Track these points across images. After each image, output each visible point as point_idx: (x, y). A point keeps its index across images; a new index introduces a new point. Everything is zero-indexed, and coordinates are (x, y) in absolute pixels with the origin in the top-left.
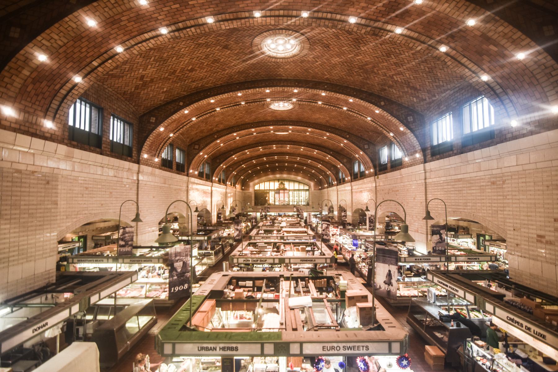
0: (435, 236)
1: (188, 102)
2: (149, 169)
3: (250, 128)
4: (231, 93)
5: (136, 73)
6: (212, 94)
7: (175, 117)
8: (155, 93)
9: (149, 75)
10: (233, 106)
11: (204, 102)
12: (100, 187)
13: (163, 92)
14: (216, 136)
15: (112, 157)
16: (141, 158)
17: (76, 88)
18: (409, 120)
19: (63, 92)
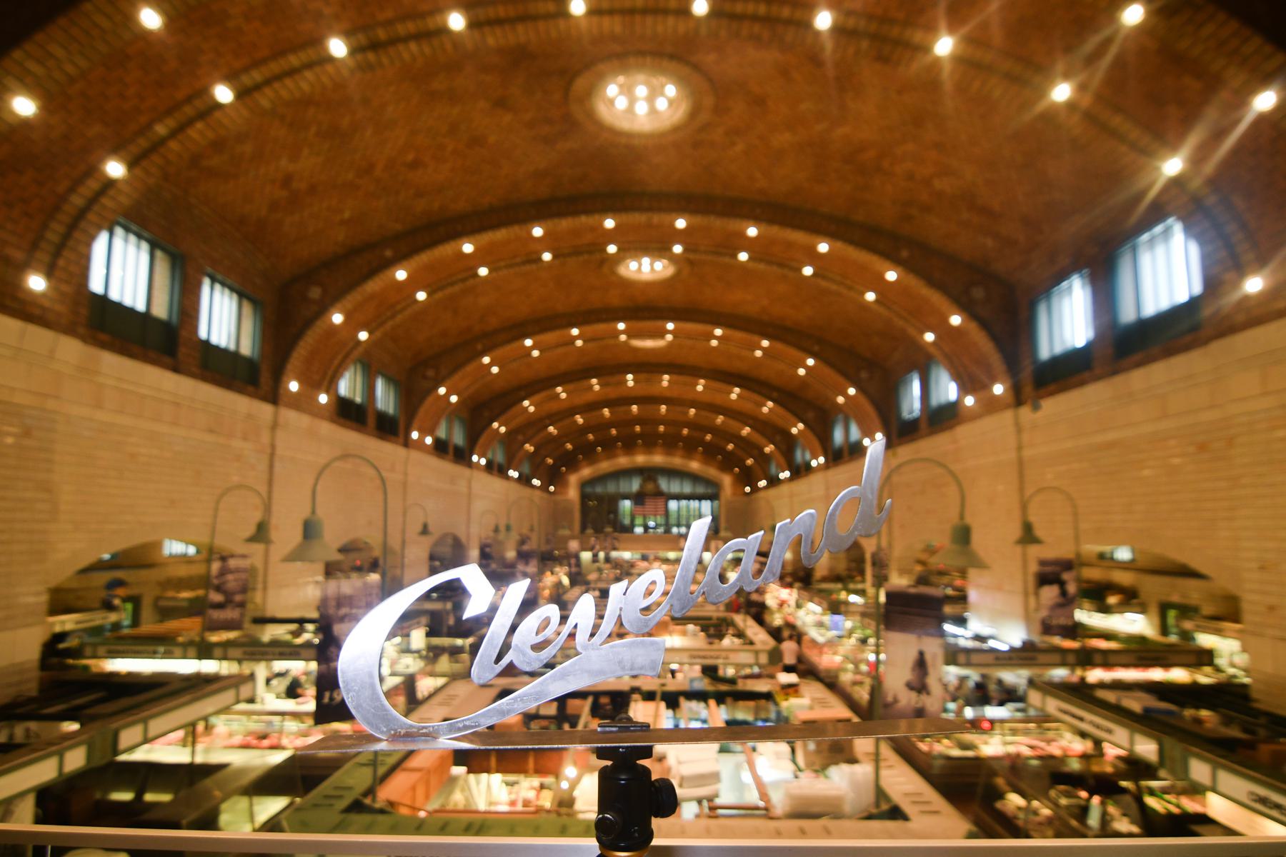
17: (112, 192)
19: (77, 200)
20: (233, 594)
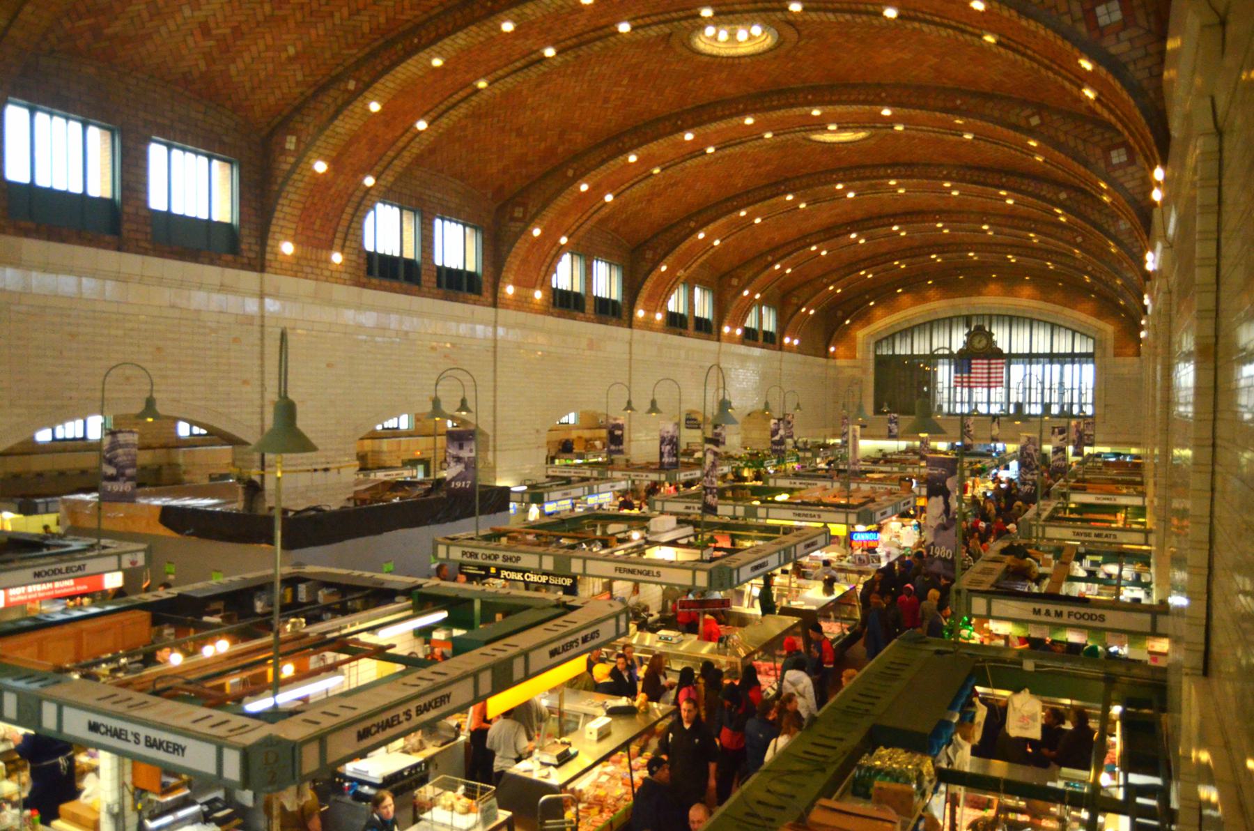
0: (933, 499)
1: (366, 78)
2: (307, 285)
3: (671, 133)
4: (473, 28)
5: (179, 20)
6: (423, 42)
7: (344, 126)
8: (270, 66)
9: (220, 17)
10: (526, 67)
11: (408, 69)
12: (120, 332)
13: (291, 60)
14: (570, 173)
15: (162, 254)
16: (268, 256)
18: (1103, 20)
20: (124, 467)
